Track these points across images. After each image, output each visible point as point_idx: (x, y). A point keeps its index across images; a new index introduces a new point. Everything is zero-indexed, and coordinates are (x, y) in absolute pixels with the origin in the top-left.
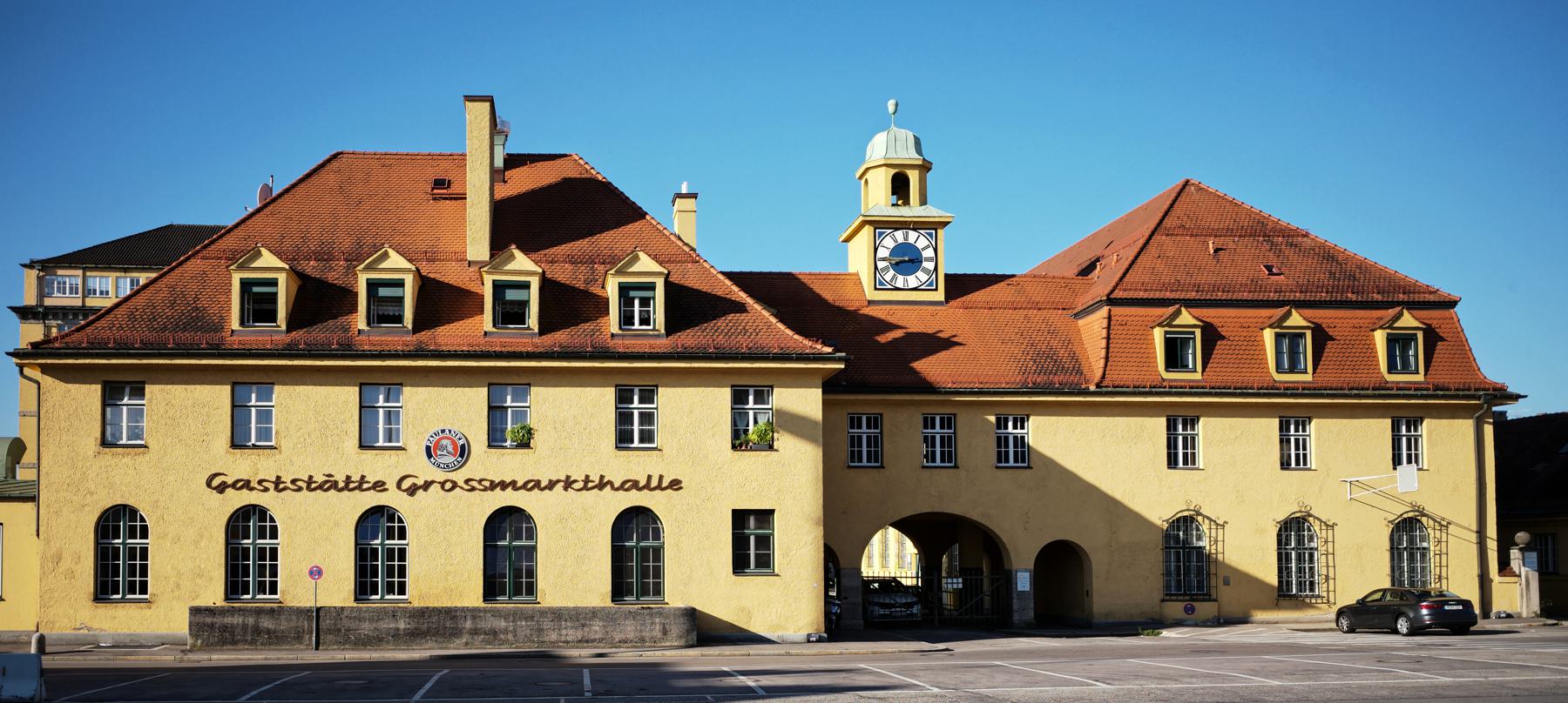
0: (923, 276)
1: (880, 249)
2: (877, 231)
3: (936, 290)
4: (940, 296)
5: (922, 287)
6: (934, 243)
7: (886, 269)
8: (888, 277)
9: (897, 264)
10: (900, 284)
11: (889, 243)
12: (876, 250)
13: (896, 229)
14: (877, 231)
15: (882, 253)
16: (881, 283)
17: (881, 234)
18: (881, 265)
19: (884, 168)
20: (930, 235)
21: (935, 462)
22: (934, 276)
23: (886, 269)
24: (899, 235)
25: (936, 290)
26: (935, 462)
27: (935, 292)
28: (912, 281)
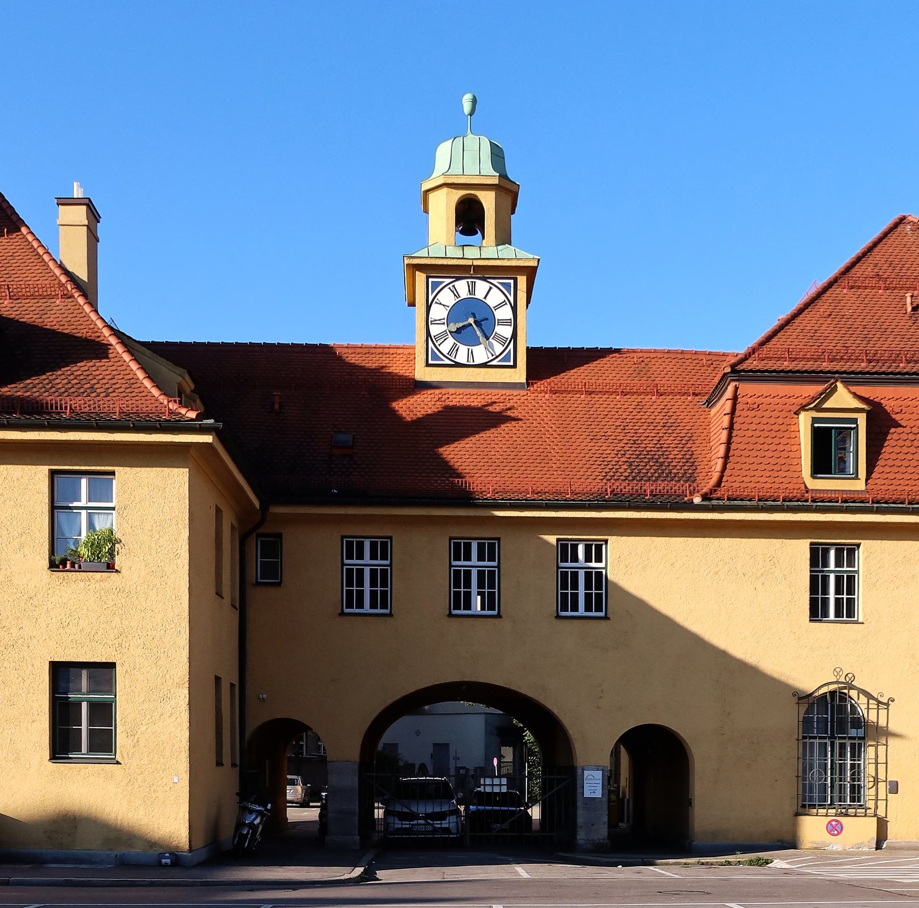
1: (434, 307)
2: (431, 280)
3: (515, 366)
4: (519, 375)
5: (494, 363)
6: (512, 299)
7: (442, 336)
8: (445, 347)
9: (459, 331)
10: (462, 358)
11: (447, 298)
12: (428, 308)
13: (458, 279)
14: (431, 280)
16: (435, 357)
17: (436, 285)
18: (435, 330)
19: (445, 190)
20: (507, 286)
23: (442, 336)
24: (462, 286)
25: (515, 366)
28: (480, 354)
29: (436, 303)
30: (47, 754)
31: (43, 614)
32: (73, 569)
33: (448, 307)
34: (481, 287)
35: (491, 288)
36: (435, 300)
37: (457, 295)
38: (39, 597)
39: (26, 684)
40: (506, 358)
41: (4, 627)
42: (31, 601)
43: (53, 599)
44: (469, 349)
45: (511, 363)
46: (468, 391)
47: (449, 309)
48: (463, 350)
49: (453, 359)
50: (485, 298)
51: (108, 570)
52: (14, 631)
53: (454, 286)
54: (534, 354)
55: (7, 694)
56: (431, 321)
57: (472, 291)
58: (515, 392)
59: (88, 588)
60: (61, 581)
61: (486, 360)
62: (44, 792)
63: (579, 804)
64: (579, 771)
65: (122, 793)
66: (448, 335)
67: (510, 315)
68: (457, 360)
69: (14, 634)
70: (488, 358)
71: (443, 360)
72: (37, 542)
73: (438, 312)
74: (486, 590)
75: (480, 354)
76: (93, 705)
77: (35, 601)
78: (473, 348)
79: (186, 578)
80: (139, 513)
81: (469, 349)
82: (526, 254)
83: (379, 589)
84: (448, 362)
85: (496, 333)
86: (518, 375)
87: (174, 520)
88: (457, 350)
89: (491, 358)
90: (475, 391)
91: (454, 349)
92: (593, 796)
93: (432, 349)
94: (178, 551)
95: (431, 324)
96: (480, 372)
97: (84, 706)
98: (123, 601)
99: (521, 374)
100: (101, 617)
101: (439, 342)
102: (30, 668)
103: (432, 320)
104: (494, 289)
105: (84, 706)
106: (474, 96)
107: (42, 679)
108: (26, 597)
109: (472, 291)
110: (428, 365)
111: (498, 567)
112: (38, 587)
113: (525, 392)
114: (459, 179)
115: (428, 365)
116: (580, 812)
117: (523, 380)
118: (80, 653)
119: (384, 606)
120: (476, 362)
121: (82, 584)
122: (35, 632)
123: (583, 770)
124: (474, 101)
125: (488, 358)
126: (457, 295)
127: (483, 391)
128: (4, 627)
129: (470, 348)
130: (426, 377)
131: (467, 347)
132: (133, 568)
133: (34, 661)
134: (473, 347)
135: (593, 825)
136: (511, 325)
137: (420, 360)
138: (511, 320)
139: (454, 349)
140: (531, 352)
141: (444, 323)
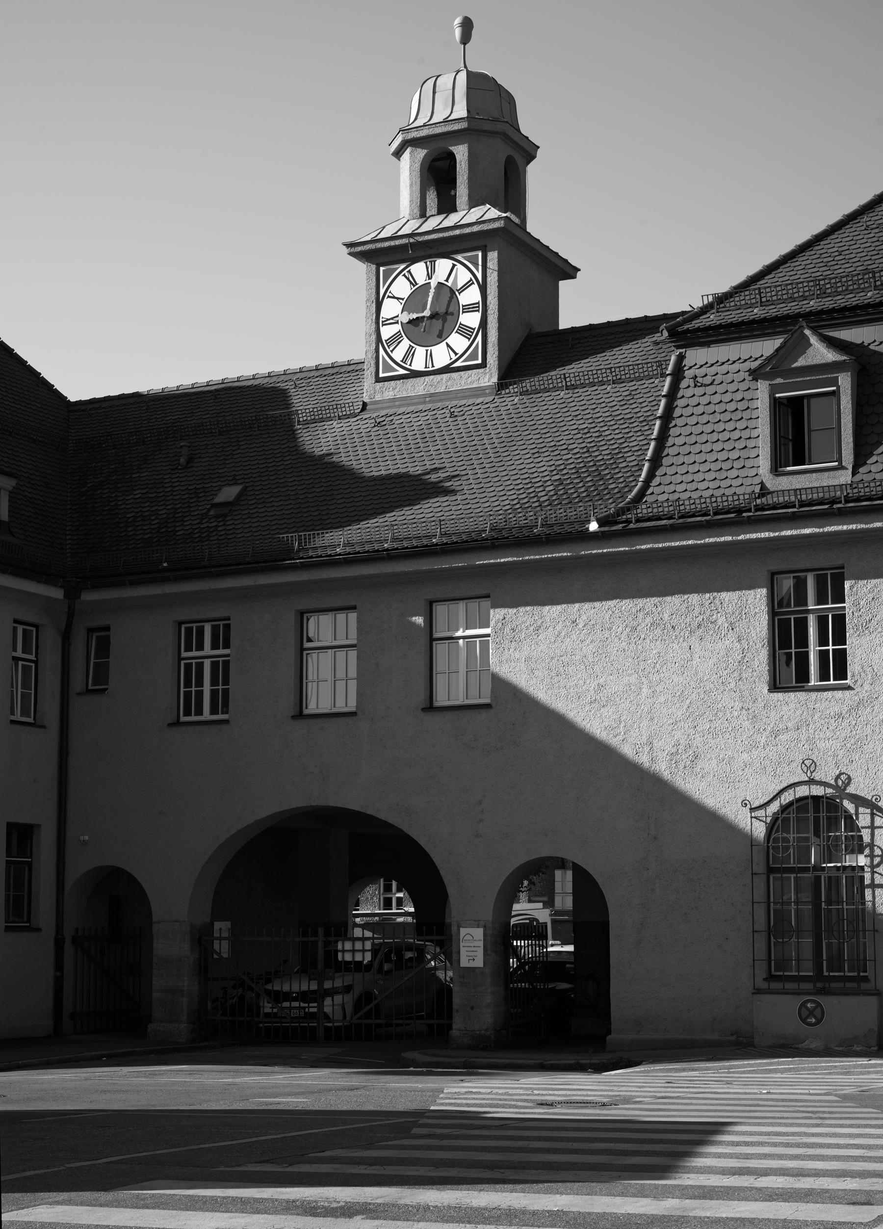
0: (459, 342)
3: (484, 365)
4: (489, 377)
5: (458, 364)
6: (479, 276)
7: (395, 339)
8: (399, 354)
10: (418, 364)
11: (401, 288)
12: (379, 305)
13: (414, 261)
15: (390, 309)
17: (387, 275)
18: (387, 332)
22: (479, 338)
23: (395, 339)
24: (419, 270)
25: (484, 365)
27: (482, 370)
28: (441, 356)
29: (389, 297)
33: (403, 299)
34: (443, 265)
35: (454, 266)
36: (388, 293)
37: (413, 283)
40: (474, 356)
44: (427, 351)
47: (403, 302)
49: (407, 366)
53: (409, 272)
56: (383, 322)
66: (402, 336)
68: (414, 367)
70: (451, 359)
75: (441, 356)
78: (433, 348)
81: (427, 351)
85: (460, 324)
89: (454, 358)
96: (442, 379)
99: (491, 374)
103: (384, 320)
104: (459, 266)
110: (378, 380)
114: (421, 132)
115: (378, 380)
125: (451, 359)
126: (413, 283)
129: (429, 348)
137: (369, 374)
138: (478, 303)
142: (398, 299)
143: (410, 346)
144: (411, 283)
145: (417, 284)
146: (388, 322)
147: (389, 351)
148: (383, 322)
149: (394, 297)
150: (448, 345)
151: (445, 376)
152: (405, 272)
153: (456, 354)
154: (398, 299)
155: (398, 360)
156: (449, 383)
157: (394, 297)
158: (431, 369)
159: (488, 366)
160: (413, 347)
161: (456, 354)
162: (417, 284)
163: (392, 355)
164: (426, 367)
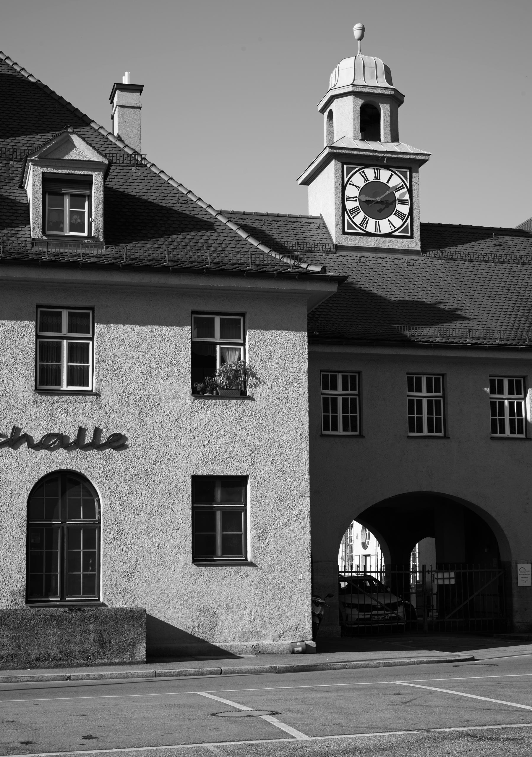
1: (349, 187)
3: (411, 237)
4: (415, 244)
5: (396, 233)
7: (355, 211)
8: (358, 219)
11: (358, 180)
16: (350, 227)
18: (349, 205)
19: (351, 97)
21: (504, 433)
23: (355, 211)
24: (370, 173)
25: (411, 237)
26: (504, 433)
28: (385, 227)
29: (350, 184)
30: (190, 557)
31: (186, 434)
32: (217, 396)
33: (360, 187)
34: (385, 175)
35: (392, 175)
36: (349, 182)
37: (366, 179)
38: (183, 419)
39: (172, 496)
40: (405, 231)
41: (153, 445)
42: (177, 423)
43: (195, 421)
45: (409, 234)
46: (379, 255)
47: (360, 189)
48: (372, 222)
49: (364, 229)
50: (388, 182)
51: (242, 396)
52: (161, 449)
53: (363, 172)
54: (425, 228)
55: (155, 505)
56: (347, 198)
57: (378, 177)
58: (415, 258)
59: (225, 411)
60: (202, 405)
61: (390, 231)
62: (187, 591)
63: (514, 592)
64: (513, 565)
65: (256, 590)
66: (360, 210)
67: (407, 197)
68: (368, 230)
69: (161, 452)
70: (391, 230)
71: (357, 230)
72: (182, 372)
73: (351, 192)
74: (415, 416)
75: (385, 227)
76: (226, 513)
77: (180, 423)
79: (307, 403)
80: (268, 348)
82: (418, 150)
83: (330, 414)
84: (360, 231)
85: (397, 210)
86: (414, 244)
87: (296, 354)
88: (367, 222)
89: (394, 229)
90: (384, 255)
91: (364, 221)
92: (525, 585)
93: (347, 220)
94: (300, 381)
95: (347, 200)
97: (219, 515)
98: (255, 423)
100: (236, 437)
101: (353, 216)
102: (176, 481)
104: (395, 176)
105: (219, 515)
106: (363, 26)
107: (185, 491)
108: (172, 419)
109: (378, 177)
111: (359, 395)
112: (182, 410)
113: (423, 258)
116: (515, 599)
117: (418, 247)
118: (219, 467)
119: (354, 429)
120: (383, 232)
121: (220, 409)
122: (180, 450)
123: (516, 564)
124: (363, 29)
125: (391, 230)
126: (366, 179)
127: (390, 256)
128: (153, 445)
129: (378, 221)
130: (343, 243)
131: (386, 220)
132: (262, 395)
133: (178, 475)
134: (380, 221)
135: (526, 609)
136: (408, 205)
137: (338, 228)
139: (364, 221)
140: (424, 227)
141: (356, 201)
142: (356, 186)
143: (365, 217)
144: (365, 179)
145: (368, 180)
146: (349, 199)
147: (351, 217)
148: (347, 198)
149: (353, 185)
150: (389, 221)
151: (388, 239)
152: (361, 171)
153: (395, 227)
154: (356, 186)
155: (358, 223)
156: (390, 244)
157: (353, 185)
158: (379, 233)
159: (414, 238)
160: (367, 218)
161: (395, 227)
162: (368, 180)
163: (354, 220)
164: (376, 231)
